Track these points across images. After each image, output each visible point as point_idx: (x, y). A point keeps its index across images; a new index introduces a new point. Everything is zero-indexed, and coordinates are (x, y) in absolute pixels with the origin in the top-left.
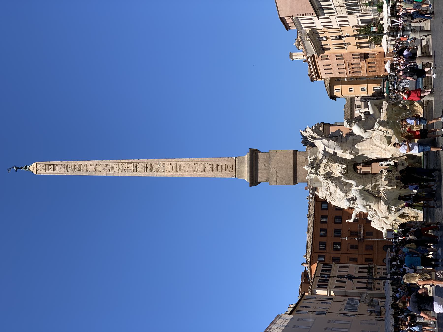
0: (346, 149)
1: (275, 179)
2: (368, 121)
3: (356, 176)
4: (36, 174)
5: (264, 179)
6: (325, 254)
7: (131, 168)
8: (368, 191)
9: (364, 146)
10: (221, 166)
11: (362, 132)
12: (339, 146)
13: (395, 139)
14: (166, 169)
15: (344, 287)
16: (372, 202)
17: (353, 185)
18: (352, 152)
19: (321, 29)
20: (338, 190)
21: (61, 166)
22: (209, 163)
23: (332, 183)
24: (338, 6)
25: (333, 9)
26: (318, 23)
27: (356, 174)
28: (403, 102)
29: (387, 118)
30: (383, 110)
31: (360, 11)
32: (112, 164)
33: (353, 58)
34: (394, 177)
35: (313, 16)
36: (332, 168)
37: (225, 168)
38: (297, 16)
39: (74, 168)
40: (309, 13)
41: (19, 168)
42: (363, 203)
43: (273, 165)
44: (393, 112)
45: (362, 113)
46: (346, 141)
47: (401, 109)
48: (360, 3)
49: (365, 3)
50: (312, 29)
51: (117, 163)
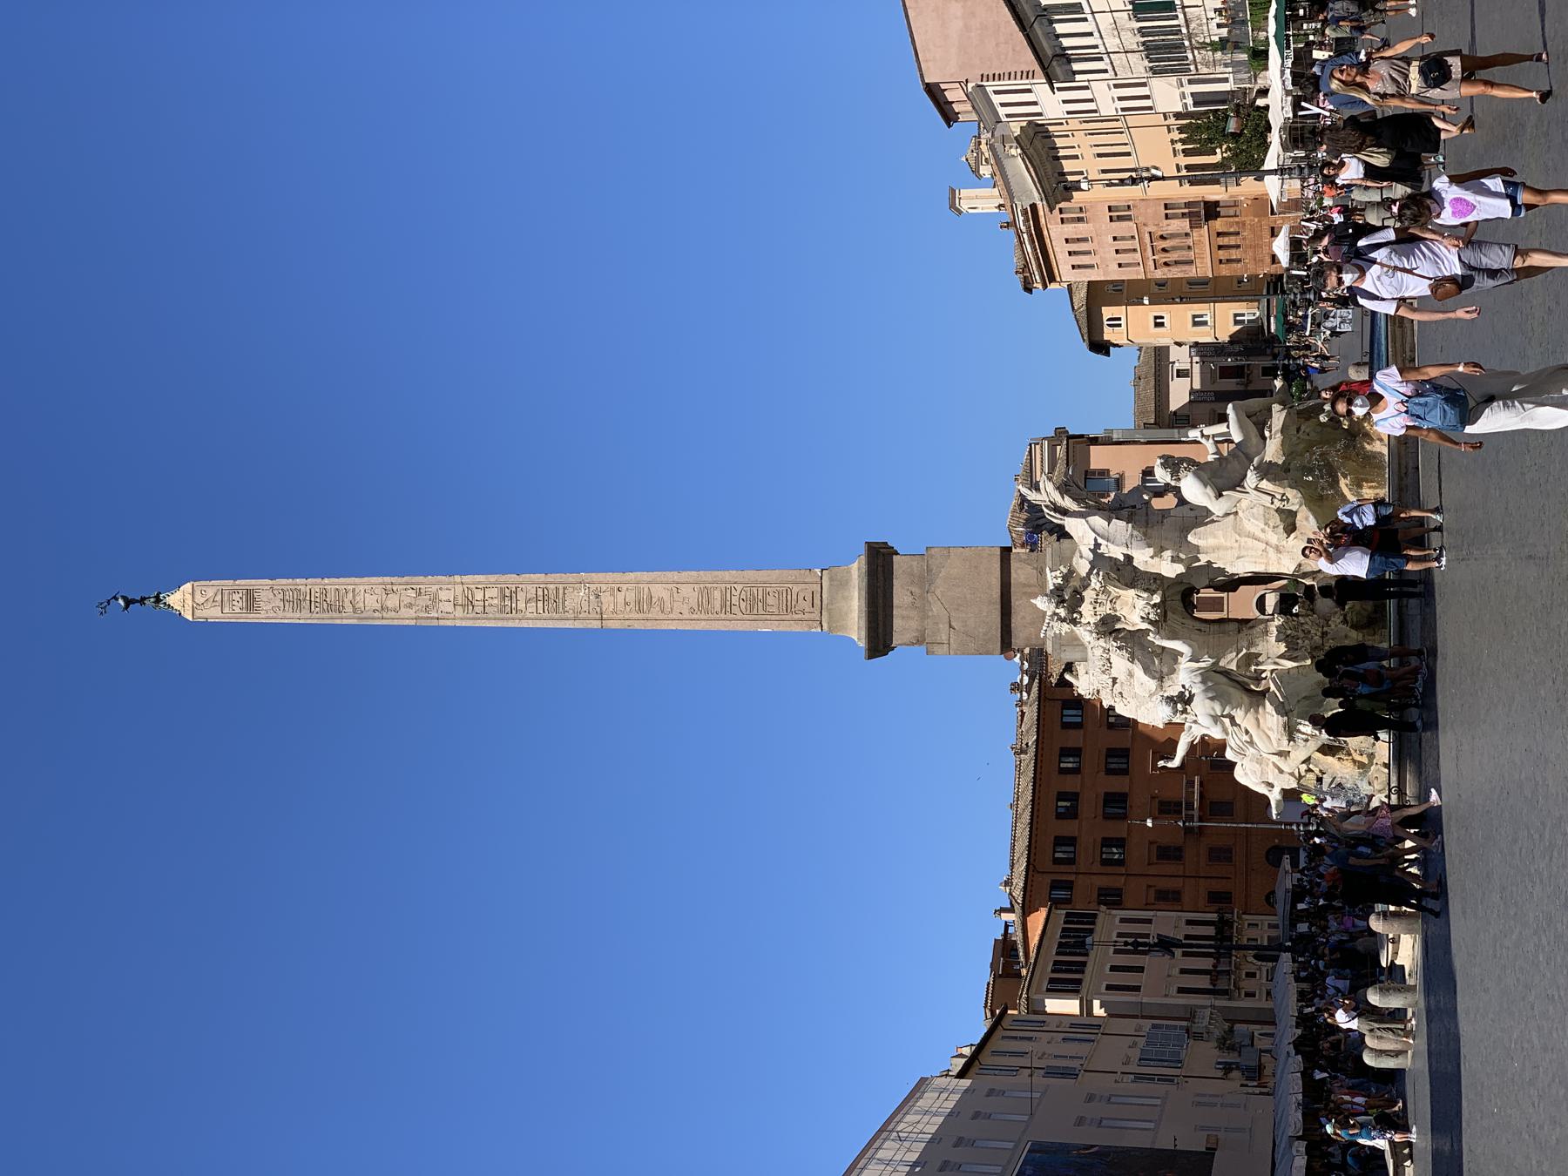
0: (1161, 547)
1: (944, 638)
2: (1227, 464)
3: (1191, 627)
4: (190, 619)
5: (910, 636)
6: (1072, 878)
7: (496, 601)
8: (1226, 673)
9: (1215, 537)
10: (776, 595)
11: (1207, 494)
12: (1139, 539)
14: (603, 606)
15: (1137, 989)
16: (1238, 706)
17: (1181, 654)
19: (1062, 124)
20: (1138, 670)
21: (271, 596)
22: (739, 587)
23: (1119, 648)
24: (1118, 50)
25: (1101, 59)
26: (1050, 103)
27: (1189, 622)
29: (1284, 454)
30: (1270, 431)
31: (1192, 67)
32: (435, 588)
33: (1167, 217)
35: (1035, 81)
36: (1118, 602)
37: (789, 604)
38: (982, 81)
39: (313, 599)
40: (1022, 72)
41: (133, 601)
42: (1213, 709)
43: (938, 592)
45: (1207, 437)
48: (1190, 42)
49: (1208, 41)
50: (1030, 122)
51: (449, 586)
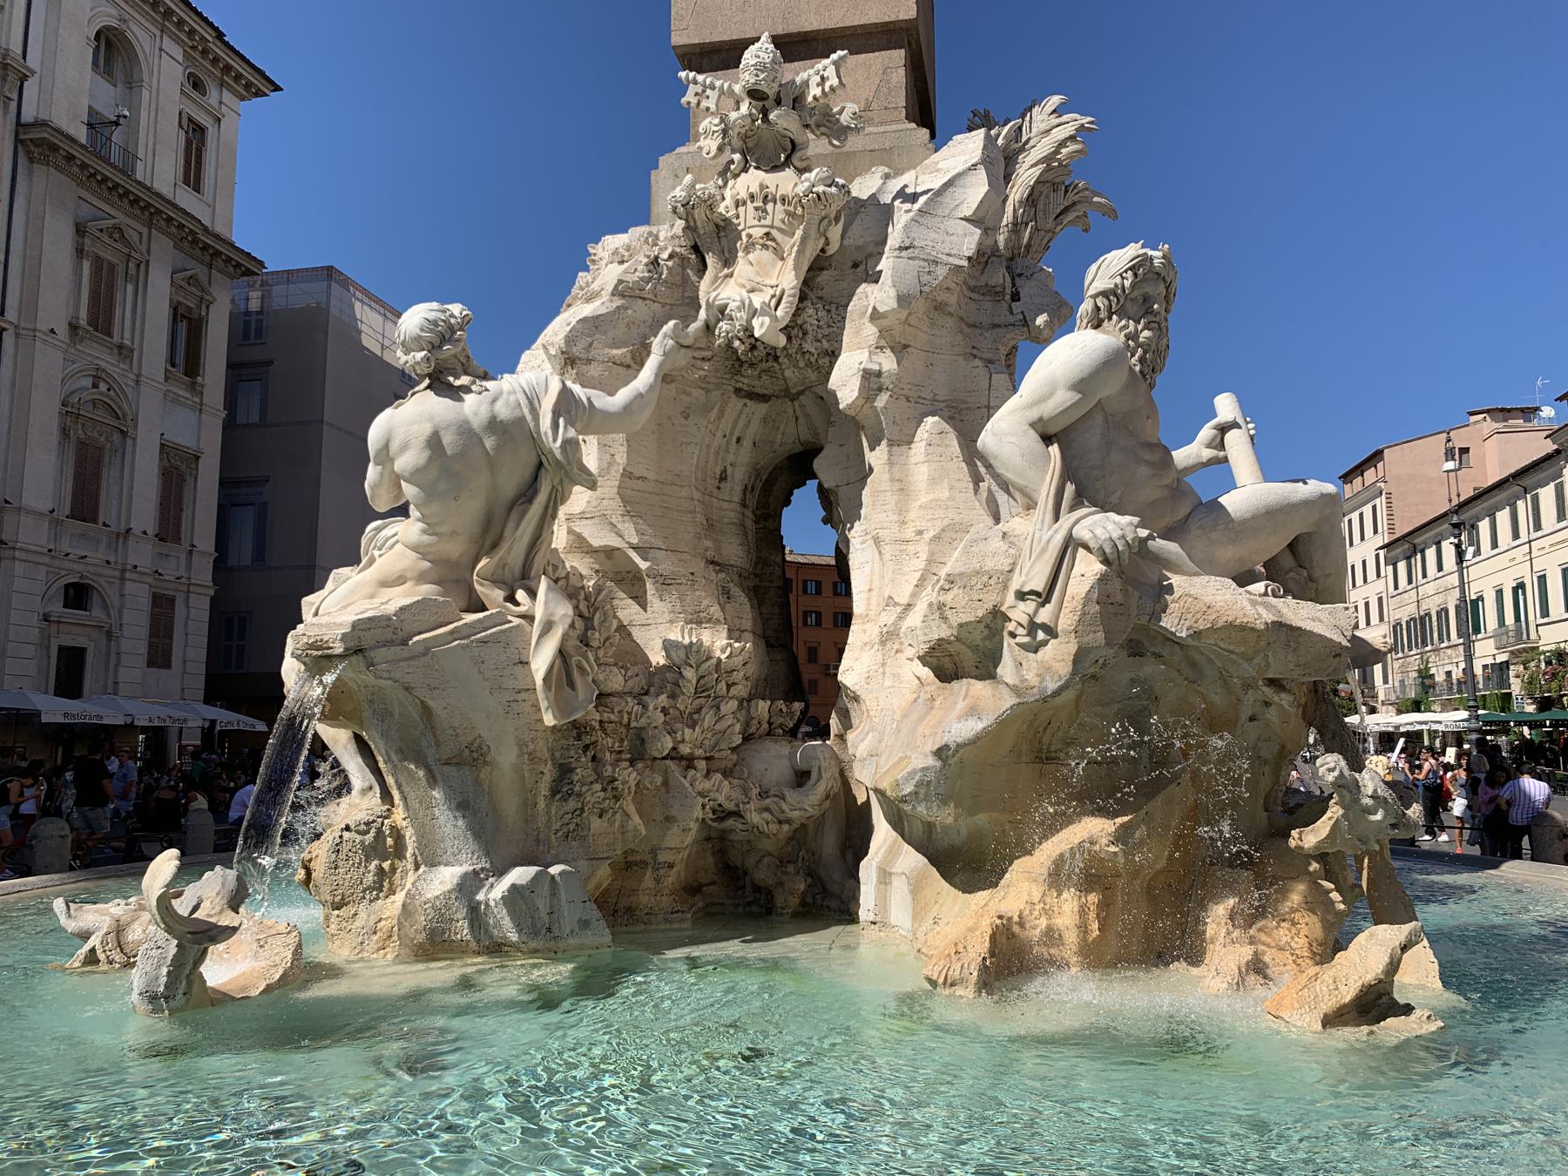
0: (906, 347)
2: (1148, 463)
3: (731, 458)
9: (933, 481)
11: (1051, 394)
12: (926, 278)
13: (973, 711)
16: (431, 527)
18: (880, 390)
23: (655, 262)
25: (1410, 582)
28: (1374, 797)
29: (1197, 634)
31: (1400, 655)
34: (699, 711)
36: (767, 255)
42: (404, 447)
44: (1250, 698)
46: (975, 356)
47: (1266, 769)
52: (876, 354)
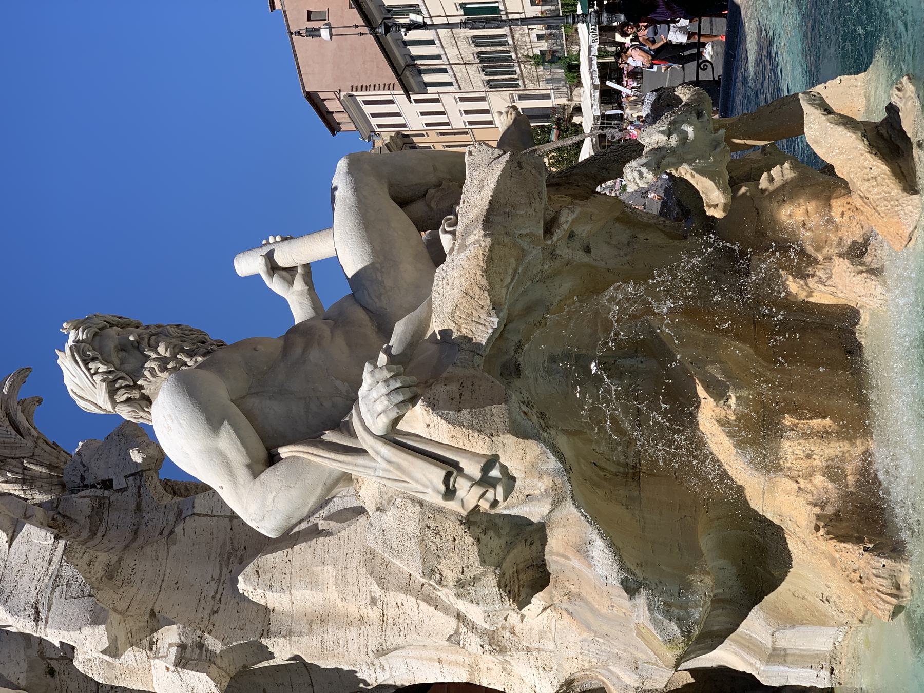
0: (153, 614)
2: (305, 350)
9: (314, 583)
12: (75, 590)
13: (583, 550)
18: (201, 646)
19: (423, 135)
24: (457, 62)
25: (445, 71)
28: (669, 134)
29: (496, 306)
31: (520, 82)
35: (395, 92)
38: (352, 91)
40: (385, 85)
44: (565, 252)
46: (172, 532)
47: (641, 236)
48: (517, 54)
49: (531, 54)
50: (398, 132)
52: (158, 651)
